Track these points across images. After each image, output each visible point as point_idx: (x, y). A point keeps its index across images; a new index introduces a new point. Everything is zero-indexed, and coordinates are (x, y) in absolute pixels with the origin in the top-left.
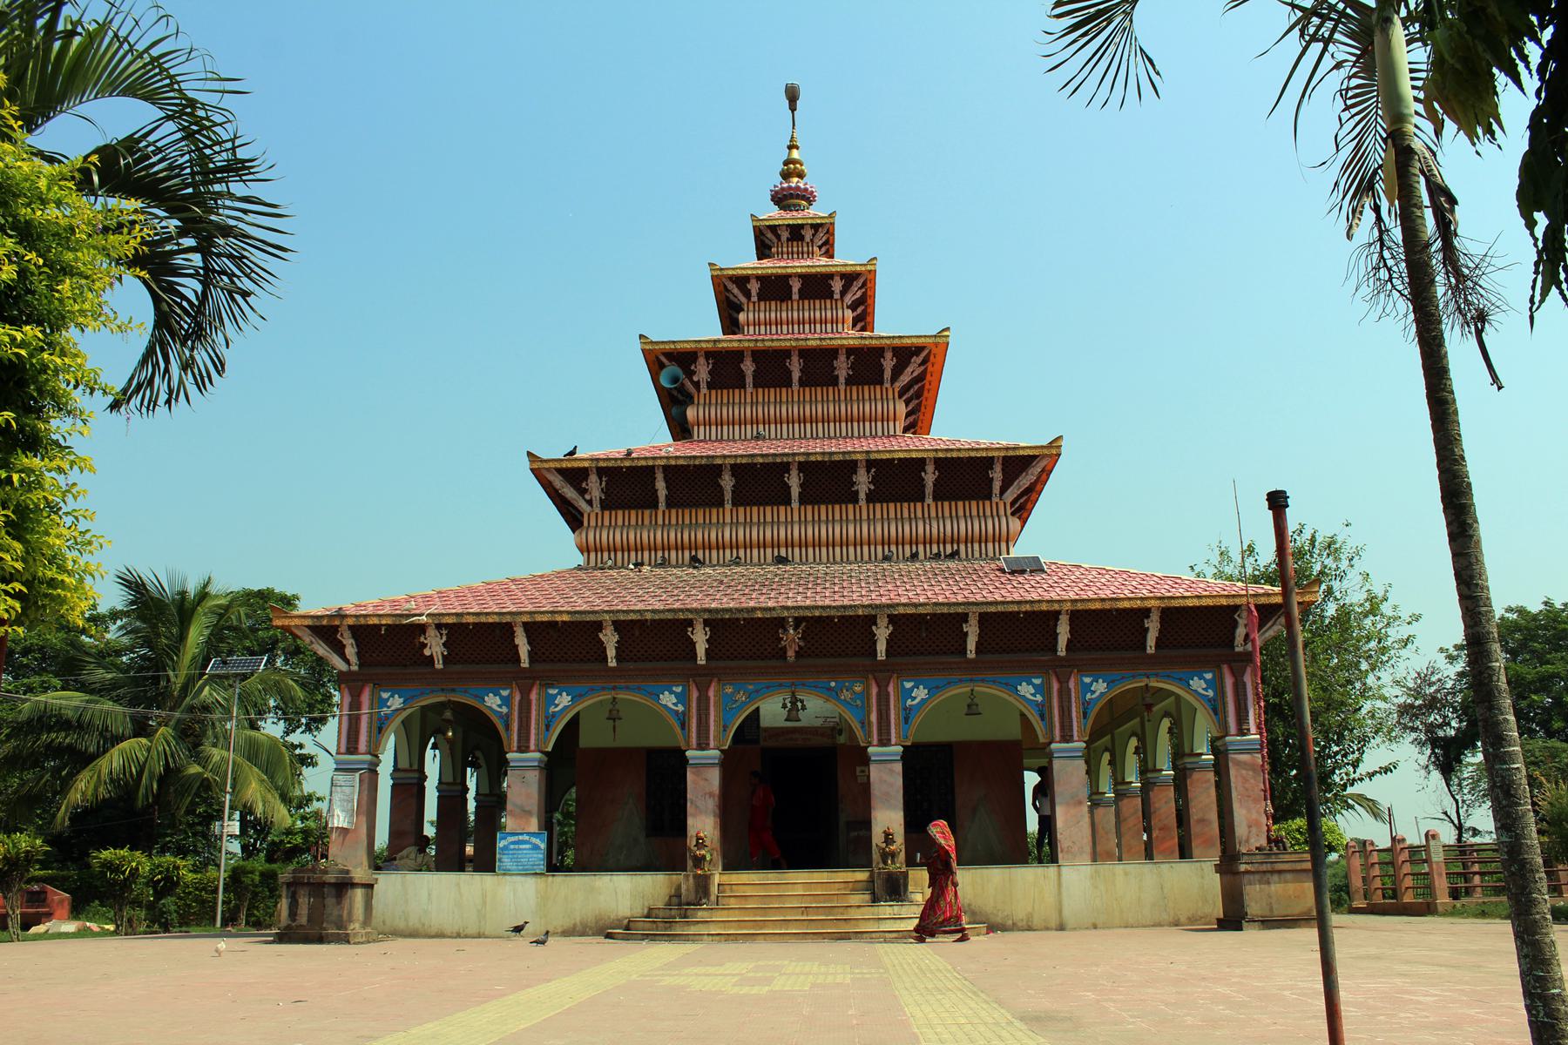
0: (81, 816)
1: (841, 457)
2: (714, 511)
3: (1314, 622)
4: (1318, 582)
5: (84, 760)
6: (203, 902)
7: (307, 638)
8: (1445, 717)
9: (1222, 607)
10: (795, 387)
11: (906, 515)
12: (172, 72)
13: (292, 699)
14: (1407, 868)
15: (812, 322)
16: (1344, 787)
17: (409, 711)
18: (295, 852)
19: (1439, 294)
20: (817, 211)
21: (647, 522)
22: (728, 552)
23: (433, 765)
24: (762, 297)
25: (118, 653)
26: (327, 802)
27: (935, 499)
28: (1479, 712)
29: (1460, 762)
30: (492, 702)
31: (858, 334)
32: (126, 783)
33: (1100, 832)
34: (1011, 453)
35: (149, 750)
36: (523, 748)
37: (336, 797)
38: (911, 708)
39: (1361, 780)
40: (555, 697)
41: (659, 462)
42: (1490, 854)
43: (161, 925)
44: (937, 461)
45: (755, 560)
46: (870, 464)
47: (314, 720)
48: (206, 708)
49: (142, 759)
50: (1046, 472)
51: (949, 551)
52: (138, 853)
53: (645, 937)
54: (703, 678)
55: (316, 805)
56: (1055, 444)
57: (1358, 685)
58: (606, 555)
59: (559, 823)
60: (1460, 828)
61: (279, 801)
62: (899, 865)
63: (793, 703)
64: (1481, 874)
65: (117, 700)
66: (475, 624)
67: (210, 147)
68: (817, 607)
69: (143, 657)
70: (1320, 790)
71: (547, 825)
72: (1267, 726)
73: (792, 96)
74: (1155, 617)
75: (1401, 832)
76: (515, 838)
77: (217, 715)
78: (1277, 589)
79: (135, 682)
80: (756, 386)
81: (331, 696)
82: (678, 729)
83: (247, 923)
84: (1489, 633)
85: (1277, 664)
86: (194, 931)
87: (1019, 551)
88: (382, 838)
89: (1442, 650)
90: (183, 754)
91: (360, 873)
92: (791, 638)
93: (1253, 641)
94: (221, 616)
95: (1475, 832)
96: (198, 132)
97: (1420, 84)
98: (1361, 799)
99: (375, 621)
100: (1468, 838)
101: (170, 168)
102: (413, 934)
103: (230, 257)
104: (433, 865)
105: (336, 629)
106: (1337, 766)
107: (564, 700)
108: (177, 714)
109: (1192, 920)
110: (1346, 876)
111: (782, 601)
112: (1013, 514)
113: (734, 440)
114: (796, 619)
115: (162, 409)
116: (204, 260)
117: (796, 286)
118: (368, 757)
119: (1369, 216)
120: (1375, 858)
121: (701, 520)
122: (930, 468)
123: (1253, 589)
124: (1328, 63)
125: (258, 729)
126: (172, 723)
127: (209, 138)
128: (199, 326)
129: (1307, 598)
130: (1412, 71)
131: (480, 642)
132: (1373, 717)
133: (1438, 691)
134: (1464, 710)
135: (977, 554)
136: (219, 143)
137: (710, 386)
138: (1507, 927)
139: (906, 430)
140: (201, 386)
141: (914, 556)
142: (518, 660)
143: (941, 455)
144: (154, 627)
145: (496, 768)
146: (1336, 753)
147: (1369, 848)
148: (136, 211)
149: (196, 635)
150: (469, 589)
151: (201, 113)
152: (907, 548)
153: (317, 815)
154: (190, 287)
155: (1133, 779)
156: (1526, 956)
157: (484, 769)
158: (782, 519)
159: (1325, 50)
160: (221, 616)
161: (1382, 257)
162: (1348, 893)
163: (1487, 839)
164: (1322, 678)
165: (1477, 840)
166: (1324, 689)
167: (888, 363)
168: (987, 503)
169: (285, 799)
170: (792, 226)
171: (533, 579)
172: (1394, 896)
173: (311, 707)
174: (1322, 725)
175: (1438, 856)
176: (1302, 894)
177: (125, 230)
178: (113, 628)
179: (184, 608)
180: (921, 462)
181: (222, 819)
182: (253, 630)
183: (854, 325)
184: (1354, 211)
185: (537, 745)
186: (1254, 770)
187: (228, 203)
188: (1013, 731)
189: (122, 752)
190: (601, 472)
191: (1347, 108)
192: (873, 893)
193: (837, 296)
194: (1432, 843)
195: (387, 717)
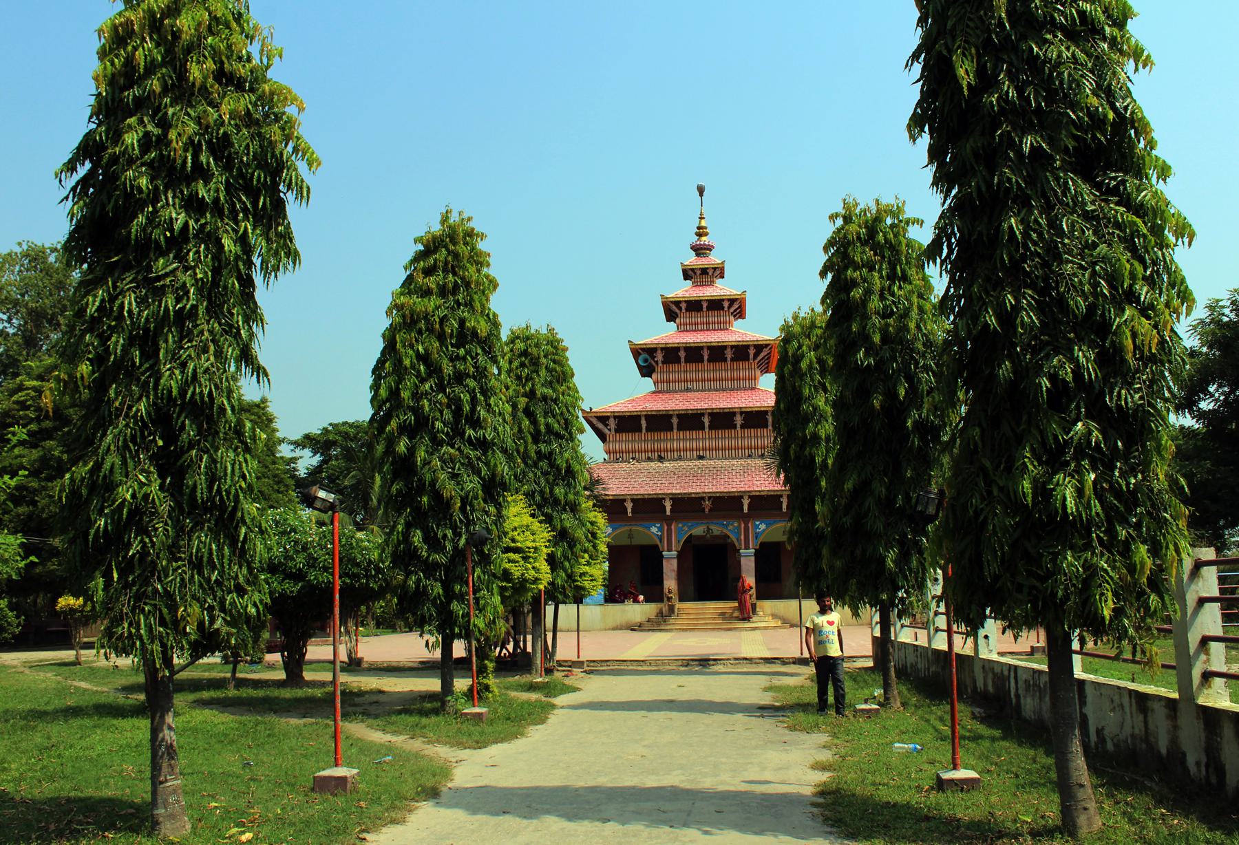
20: (714, 258)
24: (687, 310)
73: (701, 190)
92: (707, 504)
117: (705, 305)
167: (752, 352)
190: (615, 417)
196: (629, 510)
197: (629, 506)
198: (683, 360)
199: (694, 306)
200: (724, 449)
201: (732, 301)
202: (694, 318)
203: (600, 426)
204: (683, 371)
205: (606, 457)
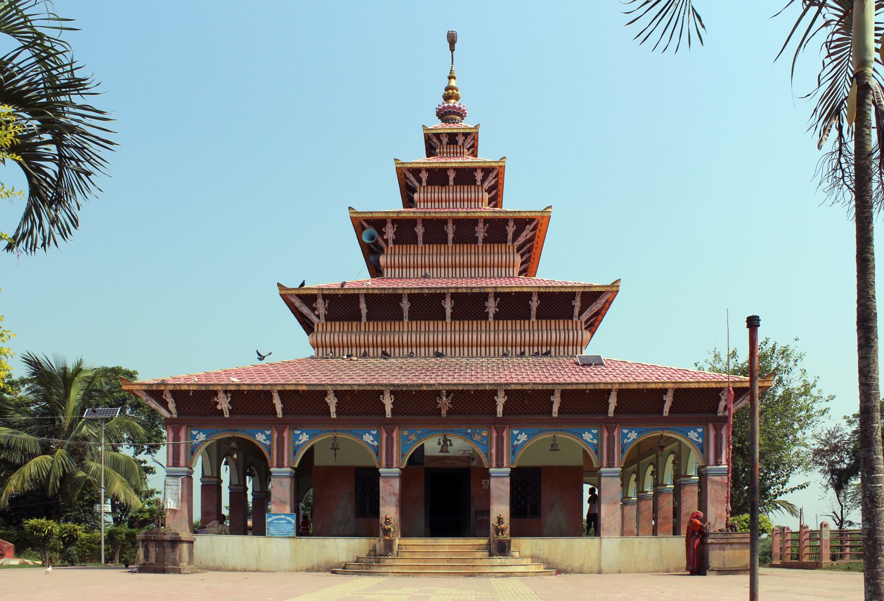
0: (15, 500)
1: (478, 290)
2: (397, 323)
3: (769, 399)
4: (774, 374)
5: (14, 468)
6: (93, 550)
7: (144, 398)
8: (842, 457)
9: (712, 389)
10: (450, 244)
11: (518, 328)
12: (25, 13)
13: (138, 434)
14: (807, 543)
15: (462, 200)
16: (776, 496)
17: (209, 442)
18: (143, 523)
19: (874, 189)
21: (354, 329)
22: (405, 349)
23: (225, 474)
25: (28, 404)
26: (162, 494)
27: (537, 318)
28: (862, 453)
29: (847, 483)
30: (261, 438)
31: (492, 210)
32: (41, 481)
33: (627, 519)
34: (587, 290)
35: (52, 462)
36: (280, 465)
37: (168, 492)
38: (516, 446)
39: (786, 492)
40: (299, 435)
41: (362, 292)
42: (858, 536)
43: (69, 562)
44: (540, 294)
45: (423, 354)
46: (497, 295)
47: (152, 446)
48: (85, 438)
49: (49, 468)
50: (609, 303)
51: (544, 351)
52: (51, 521)
53: (355, 573)
54: (388, 426)
55: (156, 496)
56: (616, 285)
57: (791, 437)
58: (329, 350)
59: (303, 509)
60: (842, 521)
61: (133, 493)
62: (506, 535)
63: (445, 441)
64: (851, 547)
65: (30, 432)
66: (248, 391)
67: (56, 69)
68: (461, 384)
69: (44, 407)
70: (760, 498)
71: (296, 510)
72: (732, 460)
74: (670, 394)
75: (806, 522)
76: (277, 517)
77: (92, 443)
78: (748, 378)
79: (40, 422)
80: (424, 243)
81: (161, 433)
82: (374, 455)
83: (120, 562)
84: (874, 406)
85: (743, 424)
86: (89, 565)
87: (588, 352)
88: (197, 516)
89: (845, 417)
90: (74, 465)
91: (185, 534)
93: (730, 409)
94: (90, 383)
95: (851, 523)
96: (47, 58)
97: (878, 38)
98: (785, 504)
99: (186, 388)
100: (846, 527)
101: (30, 83)
102: (218, 569)
103: (75, 147)
104: (228, 532)
105: (162, 392)
106: (773, 484)
107: (304, 437)
108: (68, 442)
109: (677, 570)
110: (771, 547)
111: (439, 380)
112: (586, 329)
113: (410, 278)
114: (447, 391)
115: (40, 250)
116: (59, 149)
118: (186, 469)
119: (834, 133)
120: (789, 537)
121: (389, 329)
122: (535, 298)
123: (733, 378)
124: (820, 21)
125: (118, 451)
126: (65, 447)
127: (55, 63)
128: (59, 194)
129: (766, 384)
130: (877, 29)
131: (251, 402)
132: (798, 456)
133: (839, 442)
134: (854, 454)
135: (562, 354)
136: (62, 66)
138: (861, 576)
139: (520, 273)
140: (64, 235)
141: (522, 354)
142: (276, 413)
143: (542, 290)
144: (48, 389)
145: (264, 477)
146: (773, 477)
147: (786, 531)
148: (9, 114)
149: (75, 394)
150: (244, 369)
151: (48, 44)
152: (518, 349)
153: (157, 502)
154: (51, 168)
155: (649, 489)
156: (870, 591)
157: (257, 477)
158: (440, 329)
159: (819, 12)
160: (90, 383)
161: (839, 162)
162: (771, 557)
163: (857, 528)
164: (769, 433)
165: (851, 528)
166: (770, 439)
169: (137, 492)
170: (449, 135)
171: (283, 364)
172: (798, 558)
173: (150, 439)
174: (767, 460)
175: (826, 536)
176: (742, 556)
177: (3, 127)
178: (23, 389)
179: (66, 378)
180: (530, 294)
181: (100, 503)
182: (111, 392)
183: (489, 203)
184: (825, 129)
185: (288, 464)
186: (722, 486)
187: (71, 110)
188: (577, 460)
189: (36, 463)
191: (829, 55)
192: (490, 551)
194: (824, 529)
195: (196, 445)
200: (470, 345)
203: (305, 310)
205: (312, 352)
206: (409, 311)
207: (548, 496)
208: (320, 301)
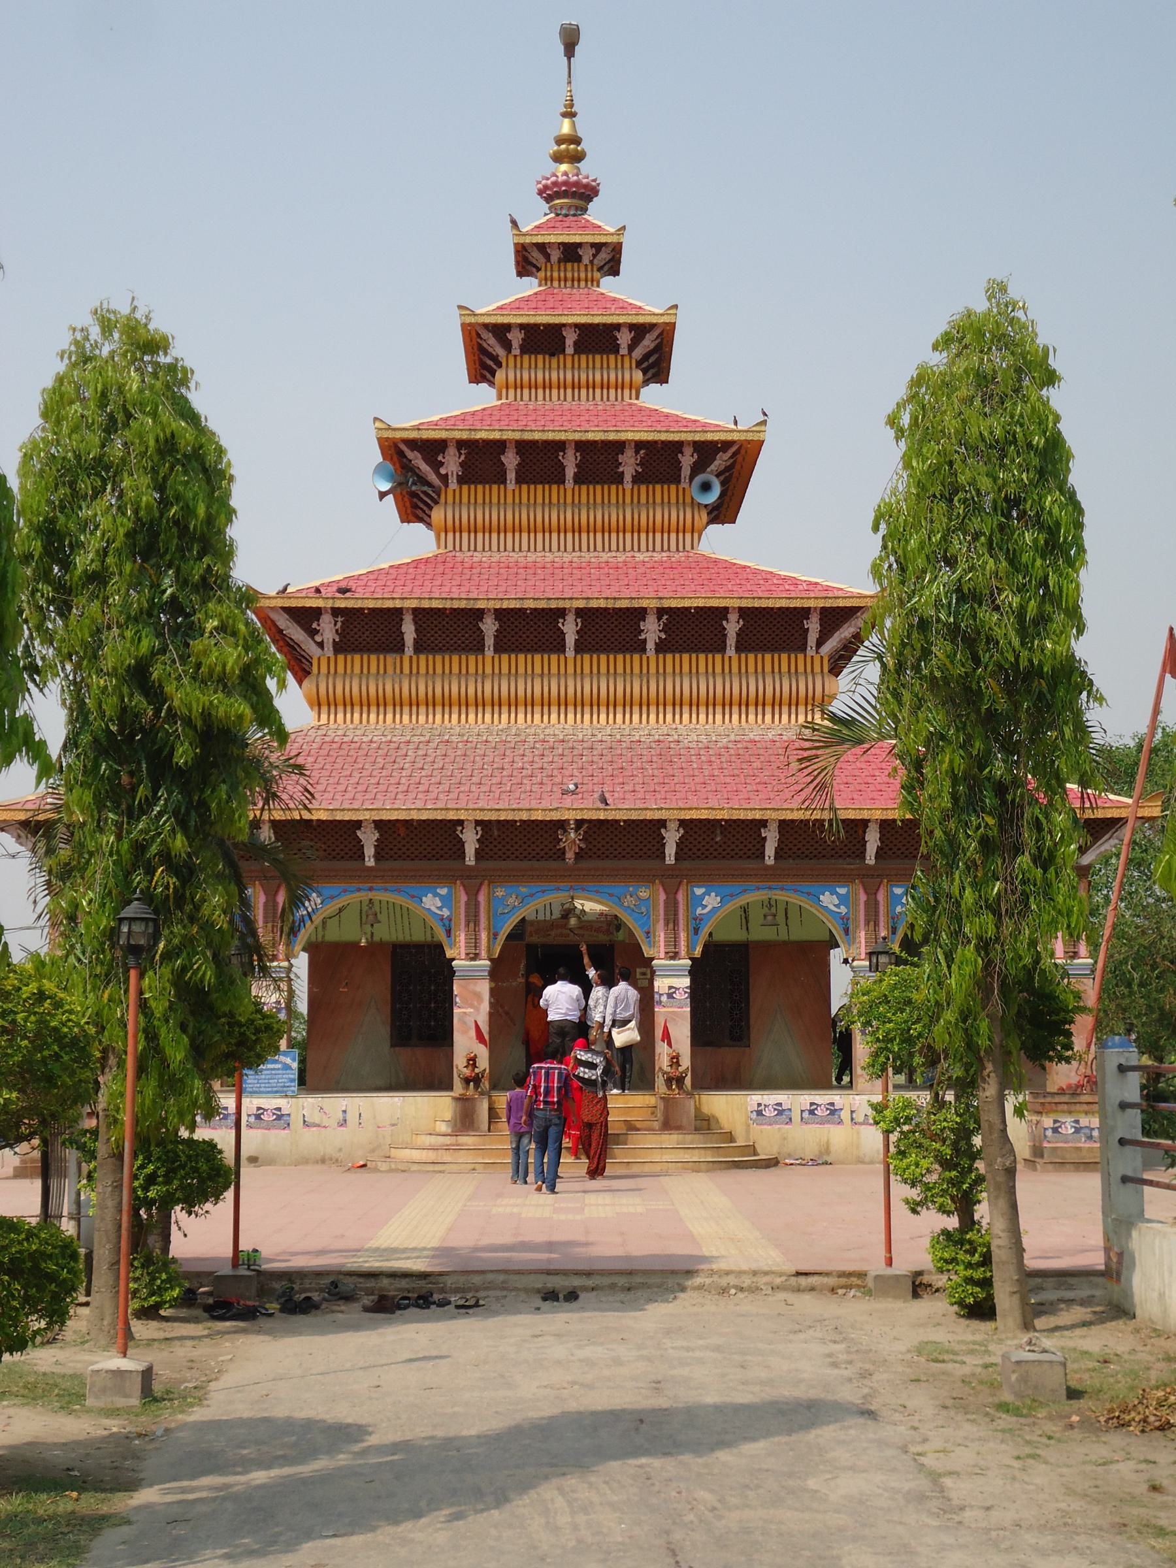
24: (526, 349)
27: (739, 649)
73: (570, 40)
117: (570, 338)
137: (461, 480)
167: (687, 460)
168: (801, 656)
193: (624, 351)
196: (369, 851)
197: (369, 839)
198: (511, 476)
199: (543, 340)
201: (639, 331)
202: (539, 369)
203: (296, 633)
204: (510, 501)
206: (496, 637)
207: (765, 999)
208: (326, 619)
